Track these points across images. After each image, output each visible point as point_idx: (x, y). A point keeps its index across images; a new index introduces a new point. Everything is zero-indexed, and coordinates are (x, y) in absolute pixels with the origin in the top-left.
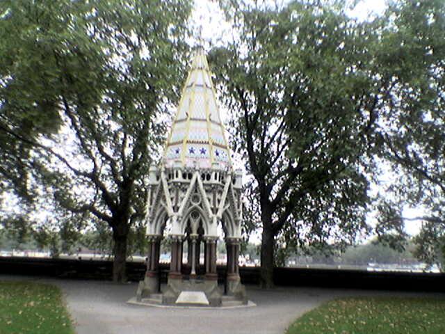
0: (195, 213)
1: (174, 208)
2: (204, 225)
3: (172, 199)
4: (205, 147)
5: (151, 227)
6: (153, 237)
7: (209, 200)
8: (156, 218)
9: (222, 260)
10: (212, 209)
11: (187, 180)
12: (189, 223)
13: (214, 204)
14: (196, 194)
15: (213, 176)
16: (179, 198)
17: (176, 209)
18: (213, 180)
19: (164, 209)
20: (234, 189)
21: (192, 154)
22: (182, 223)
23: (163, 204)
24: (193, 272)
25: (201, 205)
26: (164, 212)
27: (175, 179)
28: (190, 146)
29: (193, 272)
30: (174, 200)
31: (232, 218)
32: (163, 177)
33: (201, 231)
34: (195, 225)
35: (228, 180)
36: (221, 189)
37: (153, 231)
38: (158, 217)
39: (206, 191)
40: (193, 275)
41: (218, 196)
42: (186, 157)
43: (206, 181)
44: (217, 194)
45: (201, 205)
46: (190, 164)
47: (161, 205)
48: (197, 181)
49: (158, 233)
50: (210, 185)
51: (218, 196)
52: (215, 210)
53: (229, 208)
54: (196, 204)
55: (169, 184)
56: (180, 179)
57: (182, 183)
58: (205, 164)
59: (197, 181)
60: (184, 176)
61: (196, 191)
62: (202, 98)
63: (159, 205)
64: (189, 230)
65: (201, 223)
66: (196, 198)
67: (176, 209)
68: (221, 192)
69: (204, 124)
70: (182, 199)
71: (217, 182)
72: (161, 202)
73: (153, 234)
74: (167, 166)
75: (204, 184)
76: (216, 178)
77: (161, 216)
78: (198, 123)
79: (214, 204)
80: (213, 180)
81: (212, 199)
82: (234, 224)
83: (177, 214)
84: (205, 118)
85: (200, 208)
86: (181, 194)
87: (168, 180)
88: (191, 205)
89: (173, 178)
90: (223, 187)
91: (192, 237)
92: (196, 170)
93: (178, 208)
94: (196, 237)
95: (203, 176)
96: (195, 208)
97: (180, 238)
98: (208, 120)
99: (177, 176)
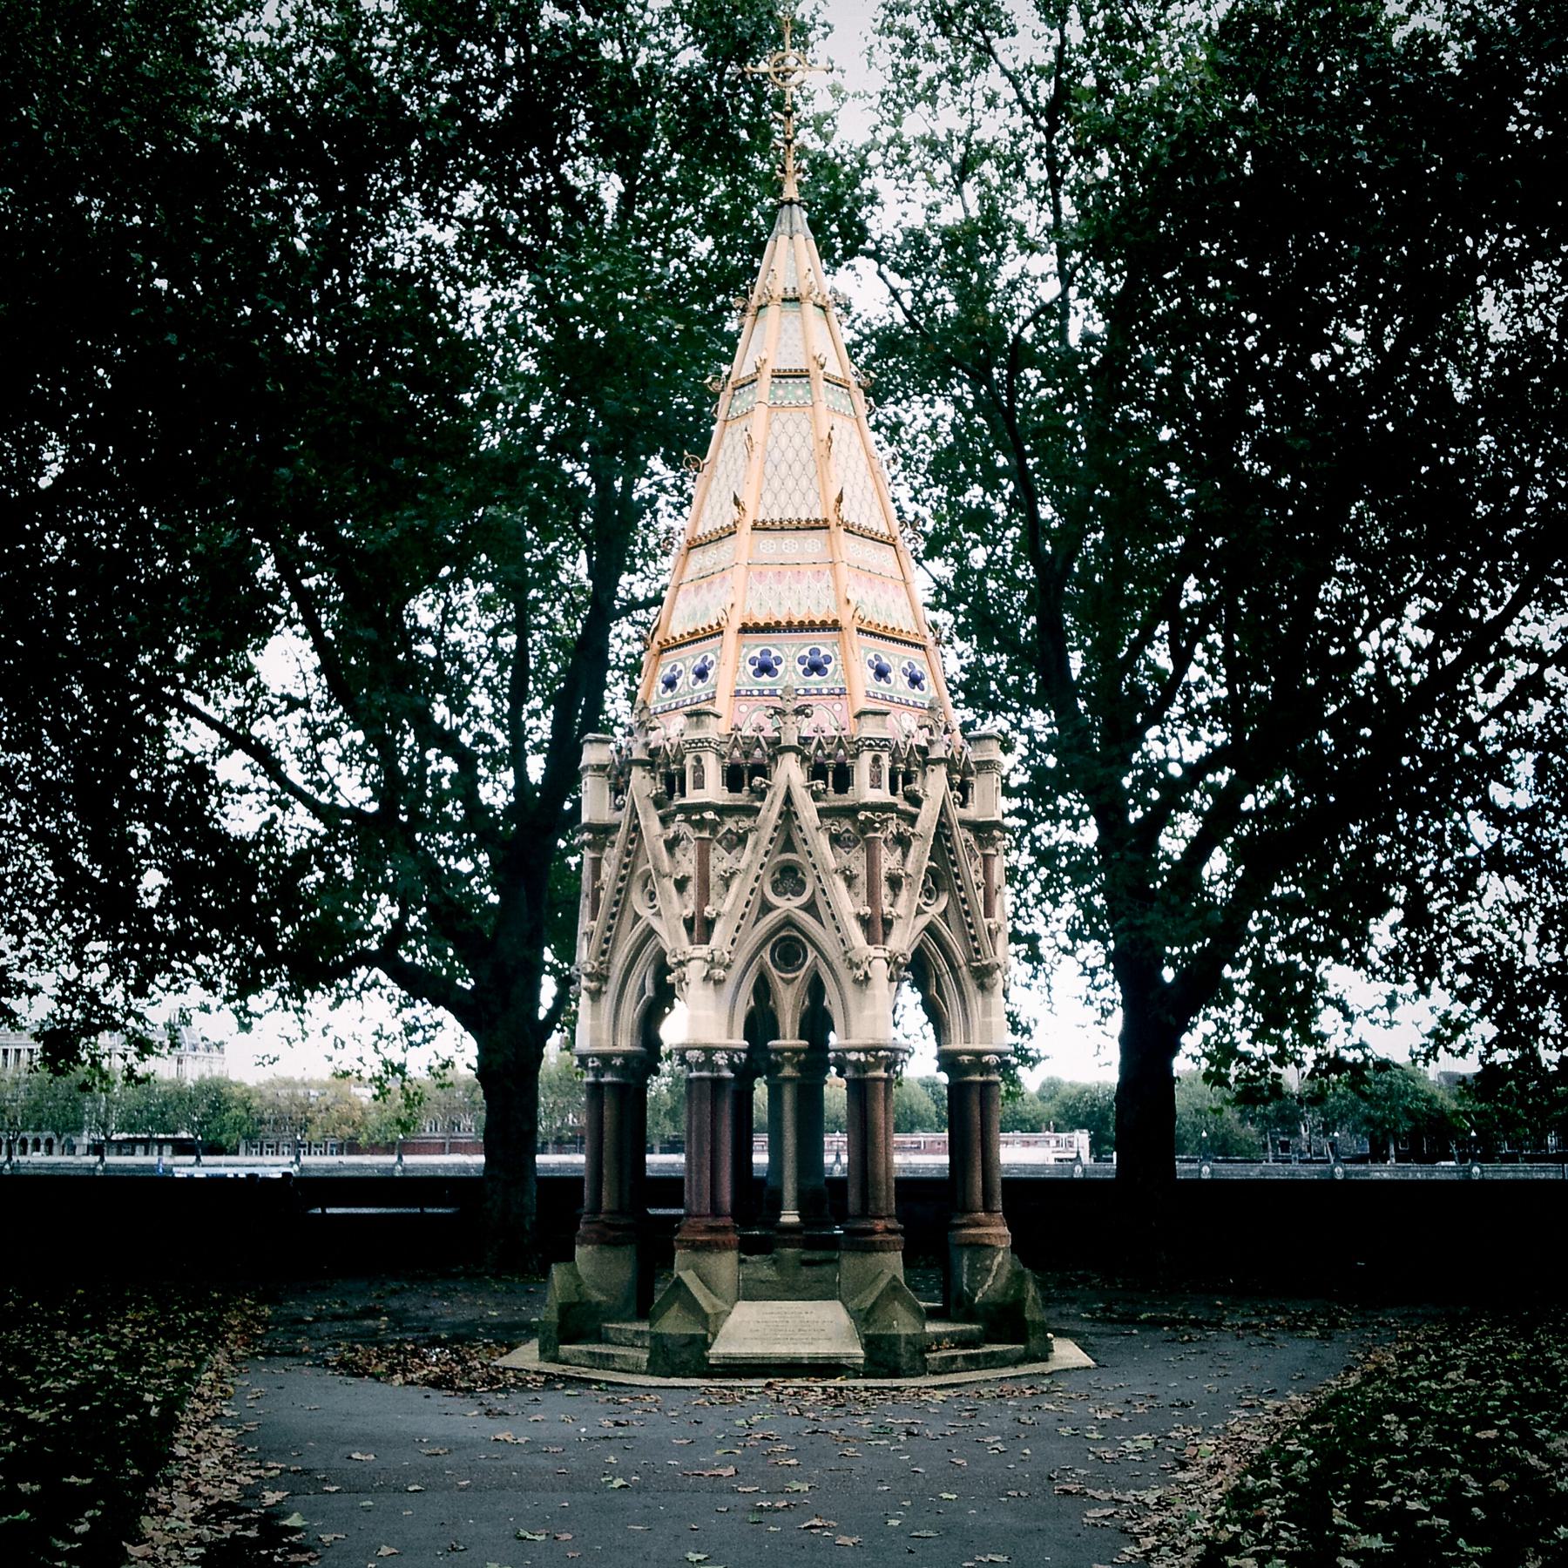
0: (788, 947)
1: (689, 924)
2: (832, 1000)
4: (824, 644)
5: (595, 1015)
6: (605, 1058)
7: (850, 880)
8: (616, 973)
9: (921, 1155)
10: (865, 922)
12: (763, 989)
13: (872, 899)
15: (862, 770)
16: (713, 878)
17: (700, 928)
18: (866, 790)
19: (650, 933)
20: (963, 823)
21: (765, 678)
22: (729, 988)
23: (646, 913)
24: (790, 1217)
25: (810, 907)
26: (649, 950)
27: (693, 796)
28: (756, 646)
29: (790, 1217)
30: (691, 888)
31: (960, 957)
32: (642, 784)
33: (816, 1022)
34: (789, 1002)
35: (935, 785)
36: (903, 826)
37: (606, 1035)
39: (835, 840)
40: (790, 1229)
41: (889, 861)
42: (737, 693)
43: (834, 800)
44: (884, 852)
45: (810, 907)
46: (753, 720)
47: (637, 917)
48: (788, 800)
49: (626, 1043)
50: (851, 812)
51: (889, 861)
52: (876, 927)
53: (944, 914)
54: (787, 905)
55: (665, 821)
56: (714, 790)
57: (722, 811)
58: (827, 720)
59: (788, 800)
60: (734, 779)
61: (789, 846)
62: (805, 426)
63: (628, 918)
64: (760, 1023)
65: (816, 988)
66: (789, 877)
68: (902, 842)
69: (813, 544)
70: (727, 882)
71: (882, 795)
72: (638, 901)
73: (606, 1047)
74: (655, 739)
75: (822, 813)
76: (876, 783)
77: (637, 971)
78: (791, 545)
79: (872, 899)
80: (866, 790)
81: (863, 878)
82: (970, 986)
83: (703, 951)
84: (818, 514)
85: (806, 919)
86: (721, 861)
87: (658, 803)
88: (766, 908)
89: (683, 795)
90: (912, 819)
91: (779, 1051)
93: (709, 924)
94: (796, 1051)
95: (817, 772)
96: (788, 922)
97: (720, 1059)
99: (699, 784)
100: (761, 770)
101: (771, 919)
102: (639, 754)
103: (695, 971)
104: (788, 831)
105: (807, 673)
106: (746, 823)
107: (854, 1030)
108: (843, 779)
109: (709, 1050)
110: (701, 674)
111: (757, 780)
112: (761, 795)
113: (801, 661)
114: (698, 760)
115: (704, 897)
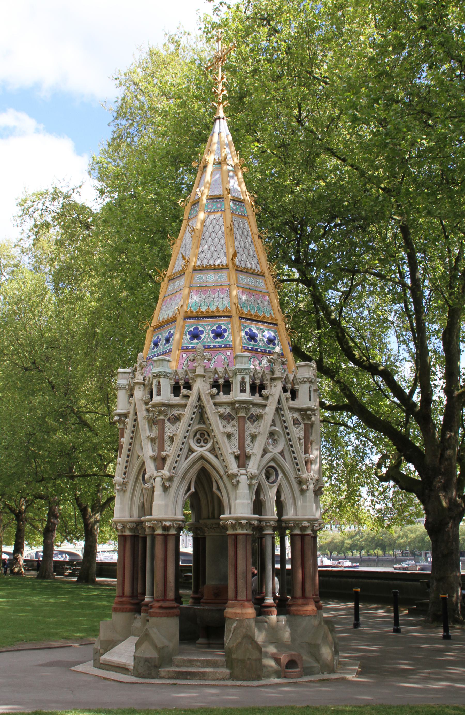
3: (229, 436)
11: (257, 399)
14: (274, 428)
17: (242, 459)
18: (303, 401)
21: (252, 342)
32: (201, 386)
38: (184, 478)
45: (282, 453)
47: (191, 451)
64: (258, 506)
67: (242, 459)
70: (253, 437)
86: (251, 428)
87: (213, 397)
92: (273, 379)
93: (248, 457)
95: (285, 390)
98: (231, 266)
100: (262, 387)
101: (268, 456)
102: (200, 371)
103: (244, 480)
104: (201, 414)
105: (215, 337)
106: (259, 411)
107: (232, 511)
108: (294, 395)
109: (249, 519)
110: (219, 334)
111: (263, 392)
112: (267, 398)
113: (213, 332)
114: (243, 379)
115: (242, 446)
